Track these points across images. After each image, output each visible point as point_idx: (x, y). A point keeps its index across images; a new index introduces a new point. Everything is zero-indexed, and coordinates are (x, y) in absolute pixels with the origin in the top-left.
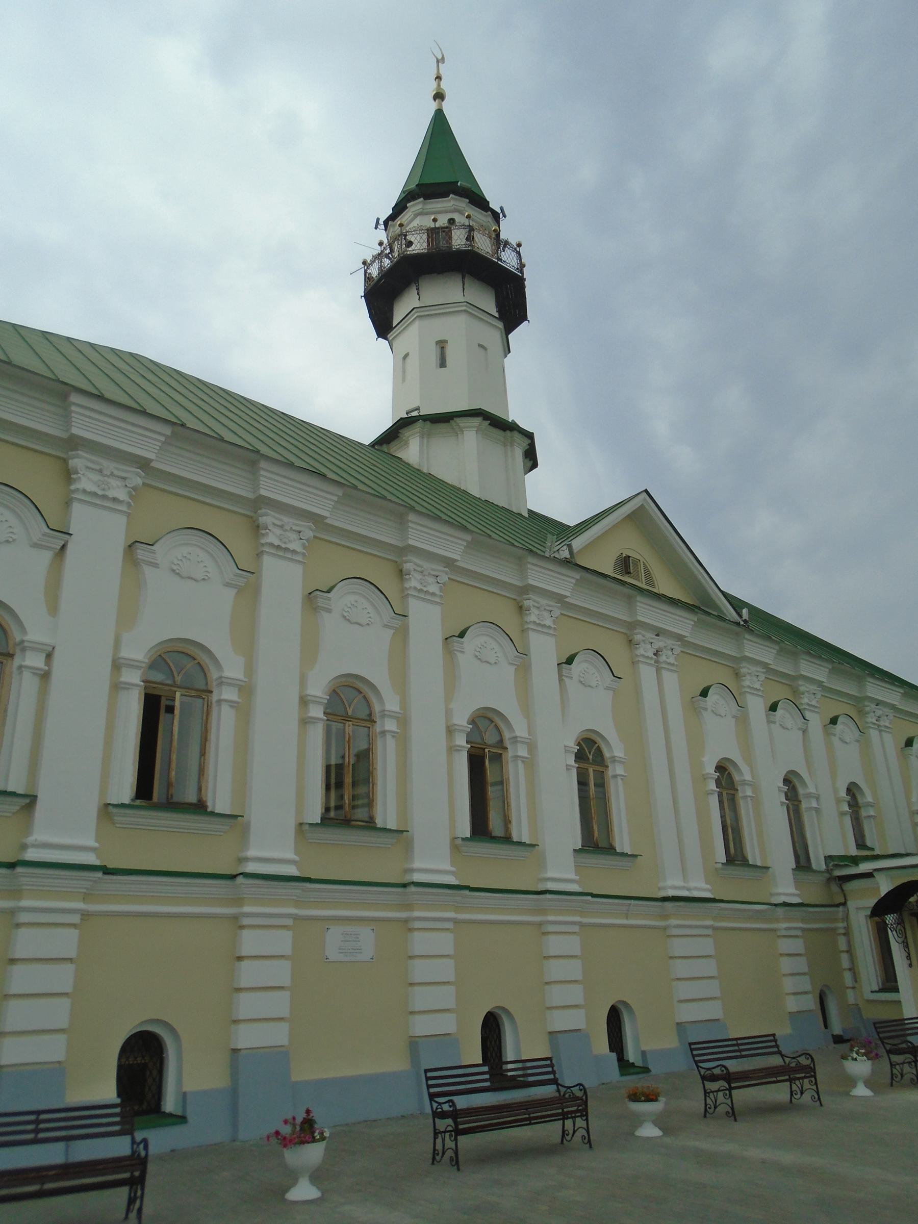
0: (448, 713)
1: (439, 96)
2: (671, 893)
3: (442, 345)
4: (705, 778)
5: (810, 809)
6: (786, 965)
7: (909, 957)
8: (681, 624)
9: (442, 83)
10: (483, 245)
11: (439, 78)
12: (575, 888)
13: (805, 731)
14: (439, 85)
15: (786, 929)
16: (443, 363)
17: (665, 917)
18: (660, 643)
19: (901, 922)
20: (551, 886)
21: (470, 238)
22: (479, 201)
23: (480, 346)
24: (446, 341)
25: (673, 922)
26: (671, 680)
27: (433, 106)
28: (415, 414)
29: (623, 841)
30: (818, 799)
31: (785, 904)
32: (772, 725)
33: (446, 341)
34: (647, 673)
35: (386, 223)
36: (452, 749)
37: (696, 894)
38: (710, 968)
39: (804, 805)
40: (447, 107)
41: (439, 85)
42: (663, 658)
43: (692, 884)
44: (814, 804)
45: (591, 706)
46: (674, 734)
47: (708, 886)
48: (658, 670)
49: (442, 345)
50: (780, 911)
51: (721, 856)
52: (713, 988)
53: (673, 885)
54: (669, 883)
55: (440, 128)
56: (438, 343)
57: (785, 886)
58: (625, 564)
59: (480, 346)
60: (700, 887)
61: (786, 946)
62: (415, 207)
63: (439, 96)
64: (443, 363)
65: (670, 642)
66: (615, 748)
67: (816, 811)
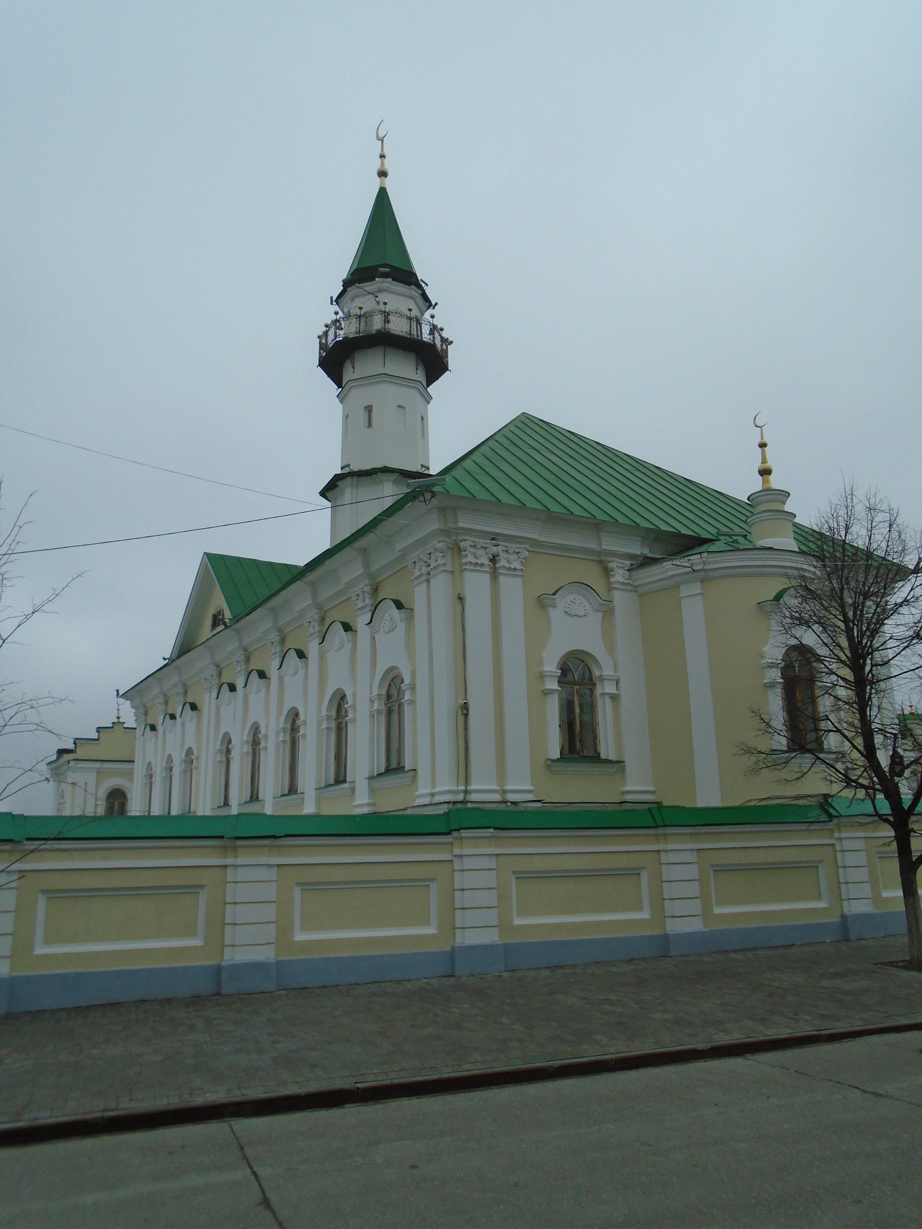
1: (383, 174)
3: (369, 409)
9: (386, 161)
10: (398, 327)
11: (382, 156)
14: (382, 164)
16: (370, 425)
21: (387, 321)
24: (371, 406)
28: (347, 470)
33: (371, 406)
35: (337, 301)
40: (390, 184)
41: (382, 164)
49: (369, 409)
56: (365, 408)
59: (399, 406)
62: (352, 291)
63: (383, 174)
64: (370, 425)
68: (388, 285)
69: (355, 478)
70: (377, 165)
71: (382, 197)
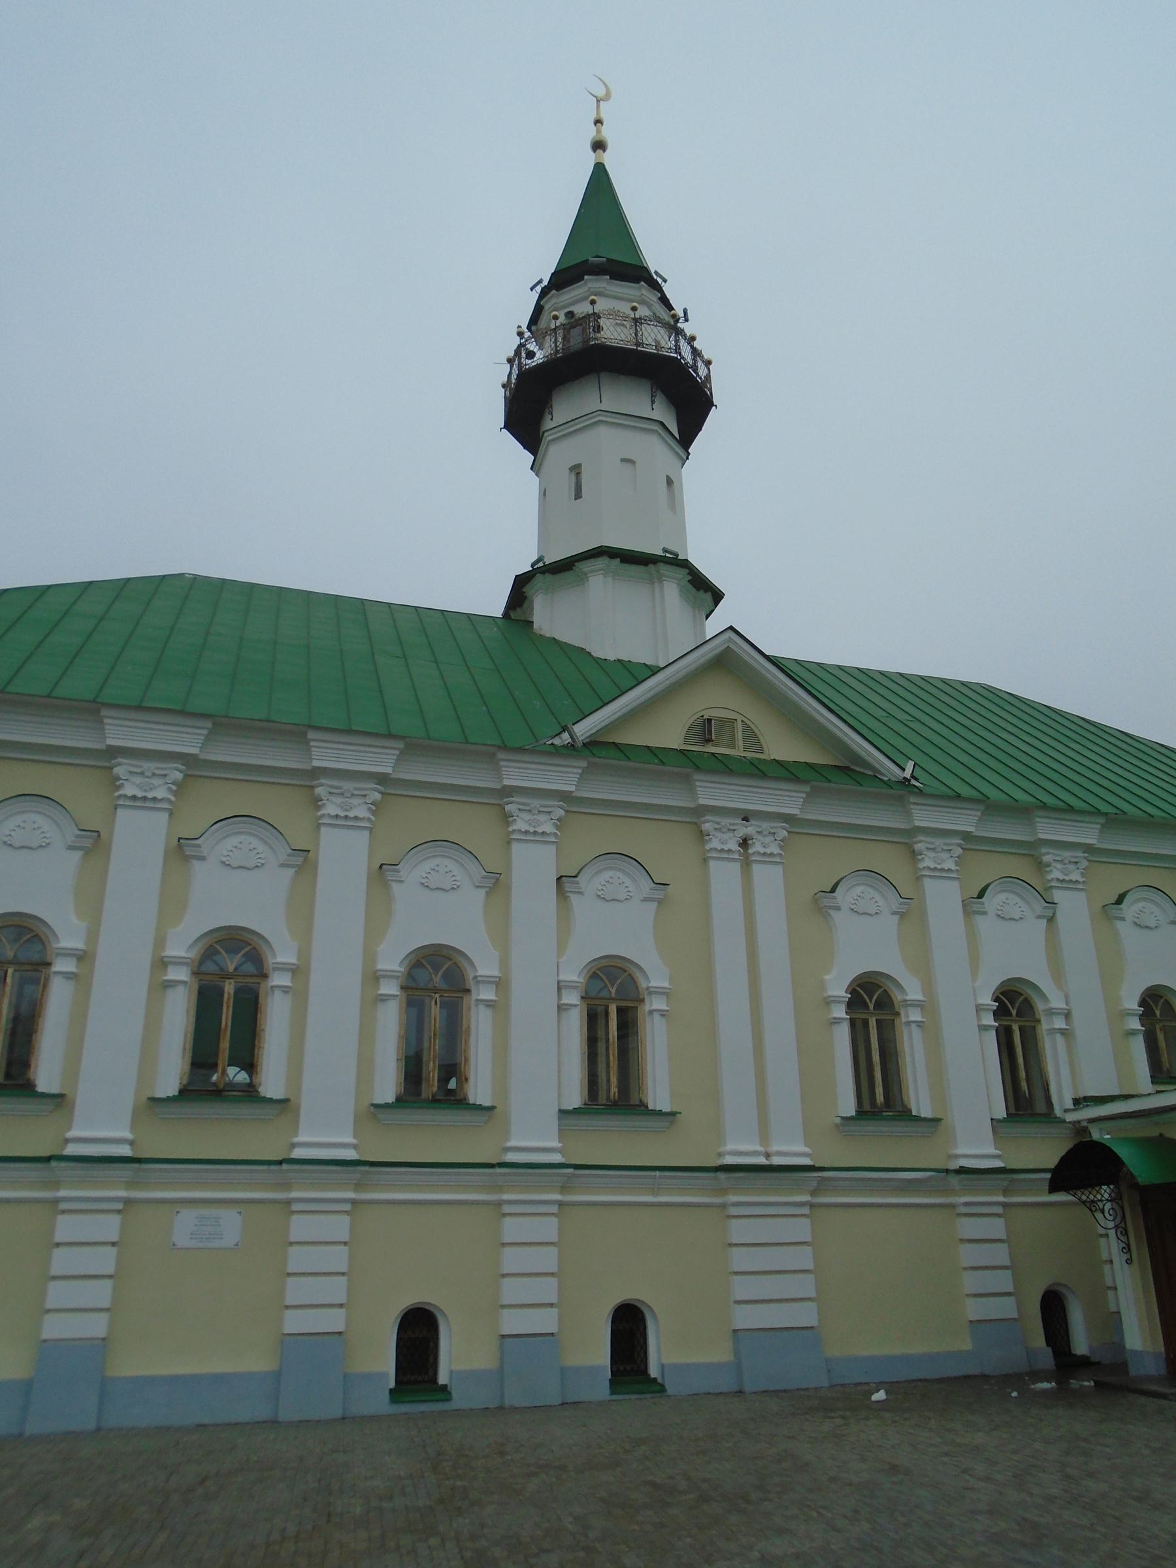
0: (369, 956)
1: (599, 145)
2: (729, 1160)
3: (576, 470)
4: (828, 1002)
5: (1052, 1031)
6: (968, 1255)
7: (1127, 1249)
8: (788, 800)
11: (598, 122)
12: (557, 1158)
13: (1051, 920)
14: (598, 132)
15: (966, 1204)
16: (578, 495)
17: (723, 1191)
18: (749, 830)
19: (1116, 1199)
20: (511, 1157)
22: (633, 272)
23: (623, 460)
25: (733, 1198)
26: (769, 880)
27: (589, 160)
29: (658, 1096)
30: (1067, 1015)
31: (963, 1171)
32: (978, 918)
34: (725, 877)
36: (372, 1001)
37: (776, 1161)
38: (804, 1258)
39: (1044, 1026)
41: (598, 132)
42: (756, 847)
43: (775, 1148)
44: (1059, 1023)
45: (618, 923)
46: (753, 952)
47: (807, 1150)
48: (746, 864)
49: (576, 470)
50: (954, 1180)
51: (849, 1107)
52: (806, 1286)
53: (741, 1147)
54: (730, 1147)
55: (600, 186)
56: (571, 469)
57: (975, 1144)
58: (705, 729)
59: (623, 460)
60: (791, 1148)
61: (969, 1228)
63: (599, 145)
64: (578, 495)
65: (766, 826)
66: (655, 975)
67: (1063, 1034)
68: (604, 285)
69: (548, 577)
70: (591, 133)
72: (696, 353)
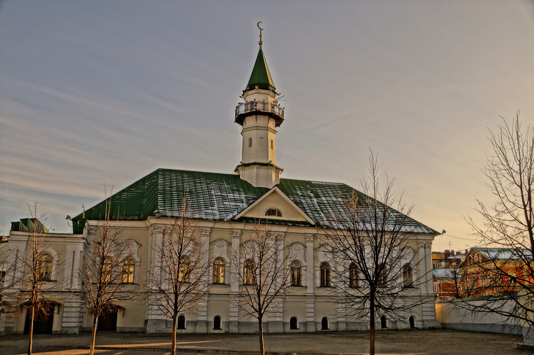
1: (261, 44)
64: (251, 146)
71: (260, 54)
72: (280, 109)
